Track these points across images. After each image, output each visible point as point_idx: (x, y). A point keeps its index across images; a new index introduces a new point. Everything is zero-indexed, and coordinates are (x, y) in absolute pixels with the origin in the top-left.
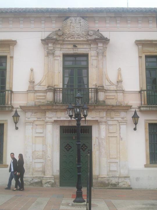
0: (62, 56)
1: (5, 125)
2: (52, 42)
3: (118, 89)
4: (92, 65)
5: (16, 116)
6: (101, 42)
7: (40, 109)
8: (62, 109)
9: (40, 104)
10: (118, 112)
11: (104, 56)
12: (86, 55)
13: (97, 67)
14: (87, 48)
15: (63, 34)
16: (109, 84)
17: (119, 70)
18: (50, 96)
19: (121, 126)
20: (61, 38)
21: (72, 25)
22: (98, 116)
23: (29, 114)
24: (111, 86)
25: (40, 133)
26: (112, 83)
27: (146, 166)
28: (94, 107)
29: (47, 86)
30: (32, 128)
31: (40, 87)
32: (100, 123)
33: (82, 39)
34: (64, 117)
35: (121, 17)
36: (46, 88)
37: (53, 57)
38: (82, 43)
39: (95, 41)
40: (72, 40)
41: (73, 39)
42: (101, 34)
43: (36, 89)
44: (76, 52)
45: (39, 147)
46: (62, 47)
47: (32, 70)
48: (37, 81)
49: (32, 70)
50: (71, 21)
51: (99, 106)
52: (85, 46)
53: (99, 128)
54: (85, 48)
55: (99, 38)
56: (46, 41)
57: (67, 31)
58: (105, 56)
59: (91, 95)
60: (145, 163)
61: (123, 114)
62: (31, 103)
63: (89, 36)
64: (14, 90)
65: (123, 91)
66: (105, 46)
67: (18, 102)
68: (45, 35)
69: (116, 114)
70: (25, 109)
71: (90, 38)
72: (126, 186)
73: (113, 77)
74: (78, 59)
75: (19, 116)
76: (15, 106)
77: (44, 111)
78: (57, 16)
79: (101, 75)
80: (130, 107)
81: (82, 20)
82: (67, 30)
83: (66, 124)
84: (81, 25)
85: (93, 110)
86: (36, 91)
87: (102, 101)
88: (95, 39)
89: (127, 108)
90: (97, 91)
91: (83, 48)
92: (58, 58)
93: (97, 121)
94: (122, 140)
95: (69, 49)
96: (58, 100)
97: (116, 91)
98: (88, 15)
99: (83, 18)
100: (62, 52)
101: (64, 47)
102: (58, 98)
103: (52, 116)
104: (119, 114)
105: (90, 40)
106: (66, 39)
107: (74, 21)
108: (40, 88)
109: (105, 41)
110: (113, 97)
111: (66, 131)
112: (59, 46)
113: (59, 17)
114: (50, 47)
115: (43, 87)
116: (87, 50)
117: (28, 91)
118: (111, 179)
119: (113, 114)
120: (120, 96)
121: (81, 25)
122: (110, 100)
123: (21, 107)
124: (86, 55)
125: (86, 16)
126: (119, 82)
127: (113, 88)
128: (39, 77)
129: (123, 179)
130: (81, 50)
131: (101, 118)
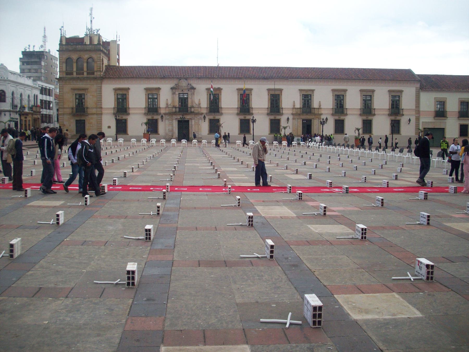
5: (162, 117)
7: (171, 114)
11: (194, 94)
18: (174, 109)
23: (166, 116)
34: (179, 117)
45: (170, 128)
51: (192, 113)
56: (172, 89)
57: (180, 85)
59: (189, 109)
61: (200, 116)
62: (167, 112)
67: (162, 111)
68: (172, 85)
70: (165, 114)
77: (172, 115)
79: (192, 102)
89: (202, 114)
90: (191, 108)
103: (175, 117)
111: (180, 122)
117: (166, 108)
119: (197, 116)
120: (199, 109)
123: (164, 114)
126: (200, 104)
127: (197, 106)
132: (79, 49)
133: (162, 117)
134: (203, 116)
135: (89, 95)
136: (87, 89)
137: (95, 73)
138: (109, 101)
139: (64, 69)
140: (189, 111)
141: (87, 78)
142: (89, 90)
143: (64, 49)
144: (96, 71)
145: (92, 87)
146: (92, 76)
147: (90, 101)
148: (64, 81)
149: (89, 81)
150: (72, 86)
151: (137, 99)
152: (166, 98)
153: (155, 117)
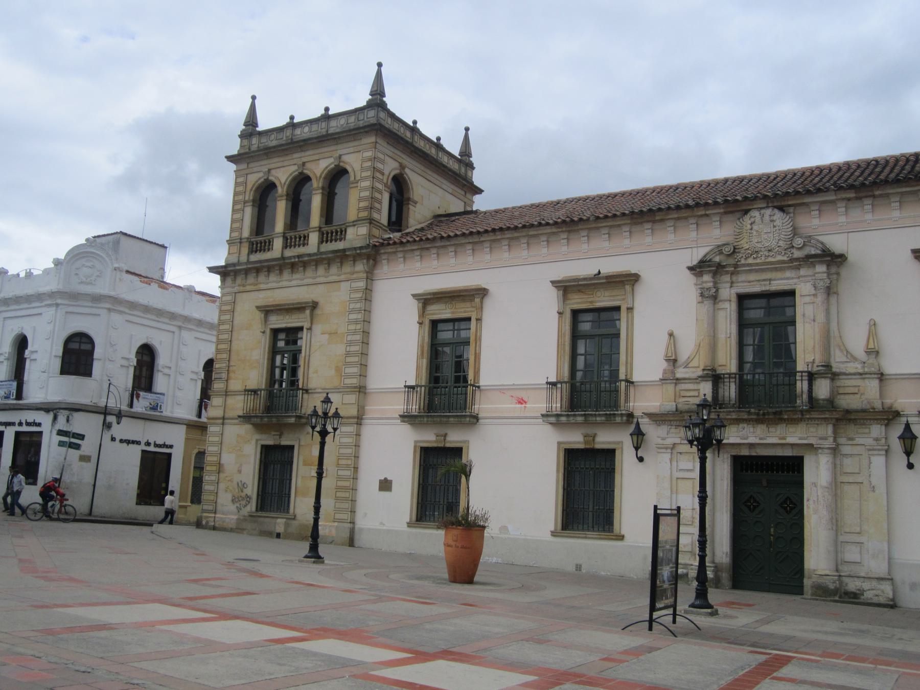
0: (734, 299)
1: (617, 453)
2: (710, 271)
3: (866, 370)
4: (804, 315)
5: (638, 435)
6: (821, 262)
8: (731, 419)
9: (686, 407)
10: (864, 424)
12: (791, 293)
13: (814, 320)
14: (793, 278)
15: (734, 252)
16: (844, 359)
17: (873, 324)
18: (706, 389)
19: (873, 459)
20: (731, 261)
21: (755, 227)
22: (815, 434)
23: (663, 430)
24: (849, 365)
25: (688, 470)
26: (852, 356)
27: (554, 534)
28: (802, 415)
29: (702, 368)
30: (671, 461)
31: (686, 370)
32: (820, 451)
33: (779, 258)
35: (874, 196)
36: (700, 373)
37: (714, 304)
38: (778, 267)
39: (809, 260)
40: (755, 261)
41: (758, 261)
42: (822, 243)
43: (678, 375)
44: (767, 288)
46: (734, 279)
47: (671, 335)
48: (683, 357)
49: (671, 335)
50: (752, 220)
52: (788, 274)
53: (818, 463)
54: (787, 279)
55: (819, 252)
56: (698, 269)
58: (836, 293)
59: (802, 386)
60: (553, 529)
61: (877, 430)
63: (794, 251)
64: (635, 378)
65: (881, 377)
66: (833, 270)
67: (644, 402)
69: (861, 431)
70: (658, 418)
71: (797, 254)
72: (882, 600)
73: (856, 342)
74: (775, 302)
75: (643, 435)
76: (637, 413)
78: (722, 211)
80: (897, 414)
81: (778, 215)
82: (745, 240)
83: (745, 452)
84: (774, 227)
85: (801, 420)
86: (678, 381)
87: (823, 400)
88: (809, 257)
90: (811, 377)
91: (782, 279)
92: (727, 305)
93: (812, 445)
94: (874, 491)
95: (749, 282)
96: (727, 399)
97: (860, 374)
98: (790, 203)
99: (781, 209)
100: (734, 291)
101: (740, 280)
102: (727, 394)
104: (867, 431)
105: (797, 259)
106: (743, 262)
107: (758, 219)
108: (687, 373)
109: (834, 260)
110: (856, 390)
112: (727, 278)
113: (726, 213)
114: (706, 282)
115: (694, 370)
116: (790, 281)
118: (846, 580)
119: (851, 430)
121: (774, 227)
122: (847, 397)
123: (650, 416)
124: (791, 293)
125: (786, 203)
126: (874, 352)
127: (852, 367)
128: (687, 346)
129: (874, 583)
130: (779, 284)
131: (821, 439)
133: (638, 435)
134: (898, 430)
135: (318, 328)
136: (314, 306)
137: (351, 232)
138: (398, 358)
140: (802, 401)
142: (318, 312)
144: (354, 224)
145: (333, 292)
147: (321, 366)
150: (262, 295)
151: (520, 344)
152: (672, 327)
153: (605, 438)
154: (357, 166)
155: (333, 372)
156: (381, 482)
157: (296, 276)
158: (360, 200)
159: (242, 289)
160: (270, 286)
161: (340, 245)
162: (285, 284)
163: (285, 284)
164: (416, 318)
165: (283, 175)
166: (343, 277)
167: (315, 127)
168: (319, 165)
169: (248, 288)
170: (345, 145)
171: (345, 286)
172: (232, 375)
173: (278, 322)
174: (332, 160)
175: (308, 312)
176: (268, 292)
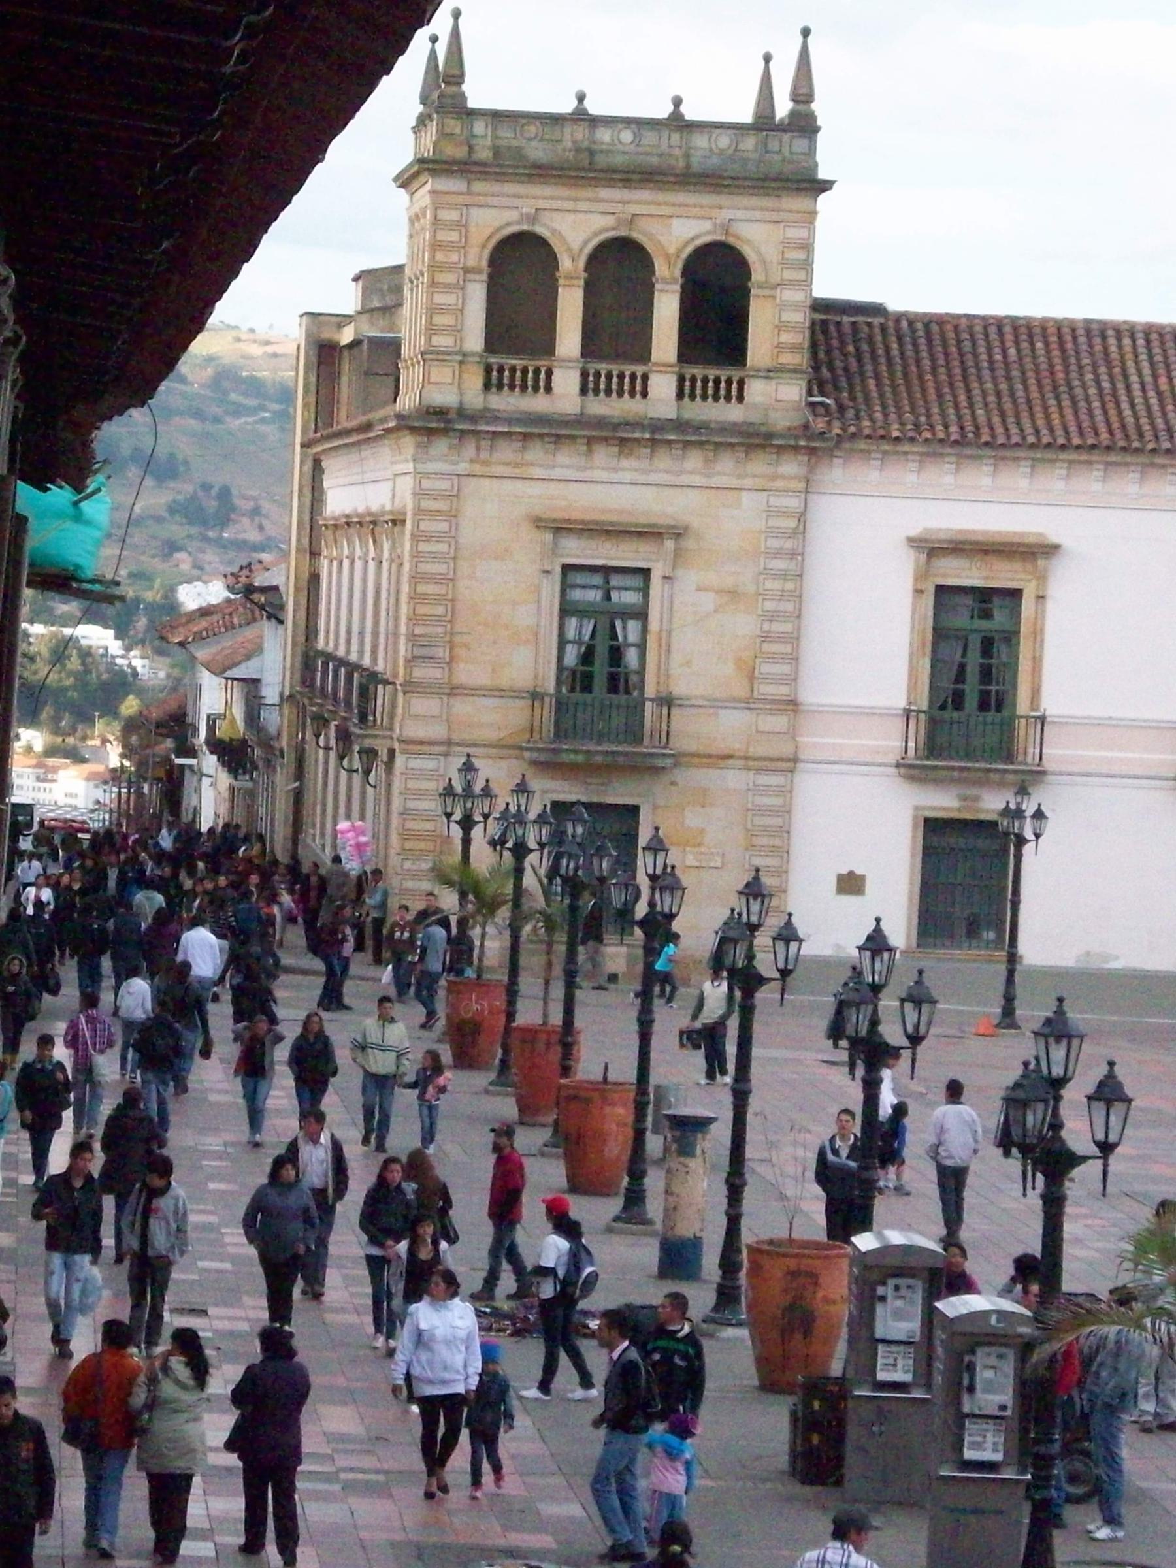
132: (619, 160)
135: (689, 578)
136: (678, 533)
137: (756, 390)
138: (867, 651)
139: (475, 341)
141: (680, 425)
142: (689, 543)
143: (484, 154)
144: (770, 373)
145: (718, 505)
146: (732, 413)
148: (469, 450)
149: (694, 460)
150: (534, 489)
154: (772, 253)
155: (729, 669)
156: (862, 878)
157: (625, 463)
158: (780, 328)
159: (477, 469)
160: (557, 473)
161: (732, 413)
162: (598, 474)
163: (598, 474)
164: (906, 583)
165: (575, 226)
166: (748, 482)
167: (650, 138)
168: (675, 231)
169: (499, 470)
170: (746, 201)
171: (747, 499)
172: (461, 652)
173: (578, 551)
174: (707, 225)
175: (670, 544)
176: (553, 489)
